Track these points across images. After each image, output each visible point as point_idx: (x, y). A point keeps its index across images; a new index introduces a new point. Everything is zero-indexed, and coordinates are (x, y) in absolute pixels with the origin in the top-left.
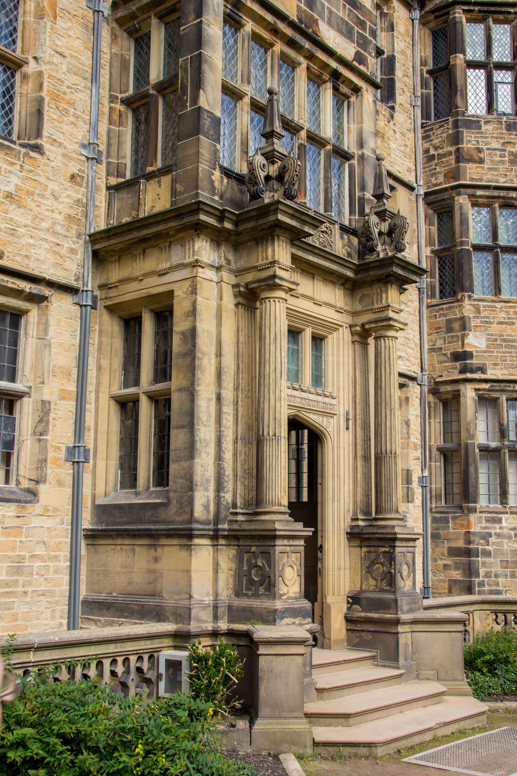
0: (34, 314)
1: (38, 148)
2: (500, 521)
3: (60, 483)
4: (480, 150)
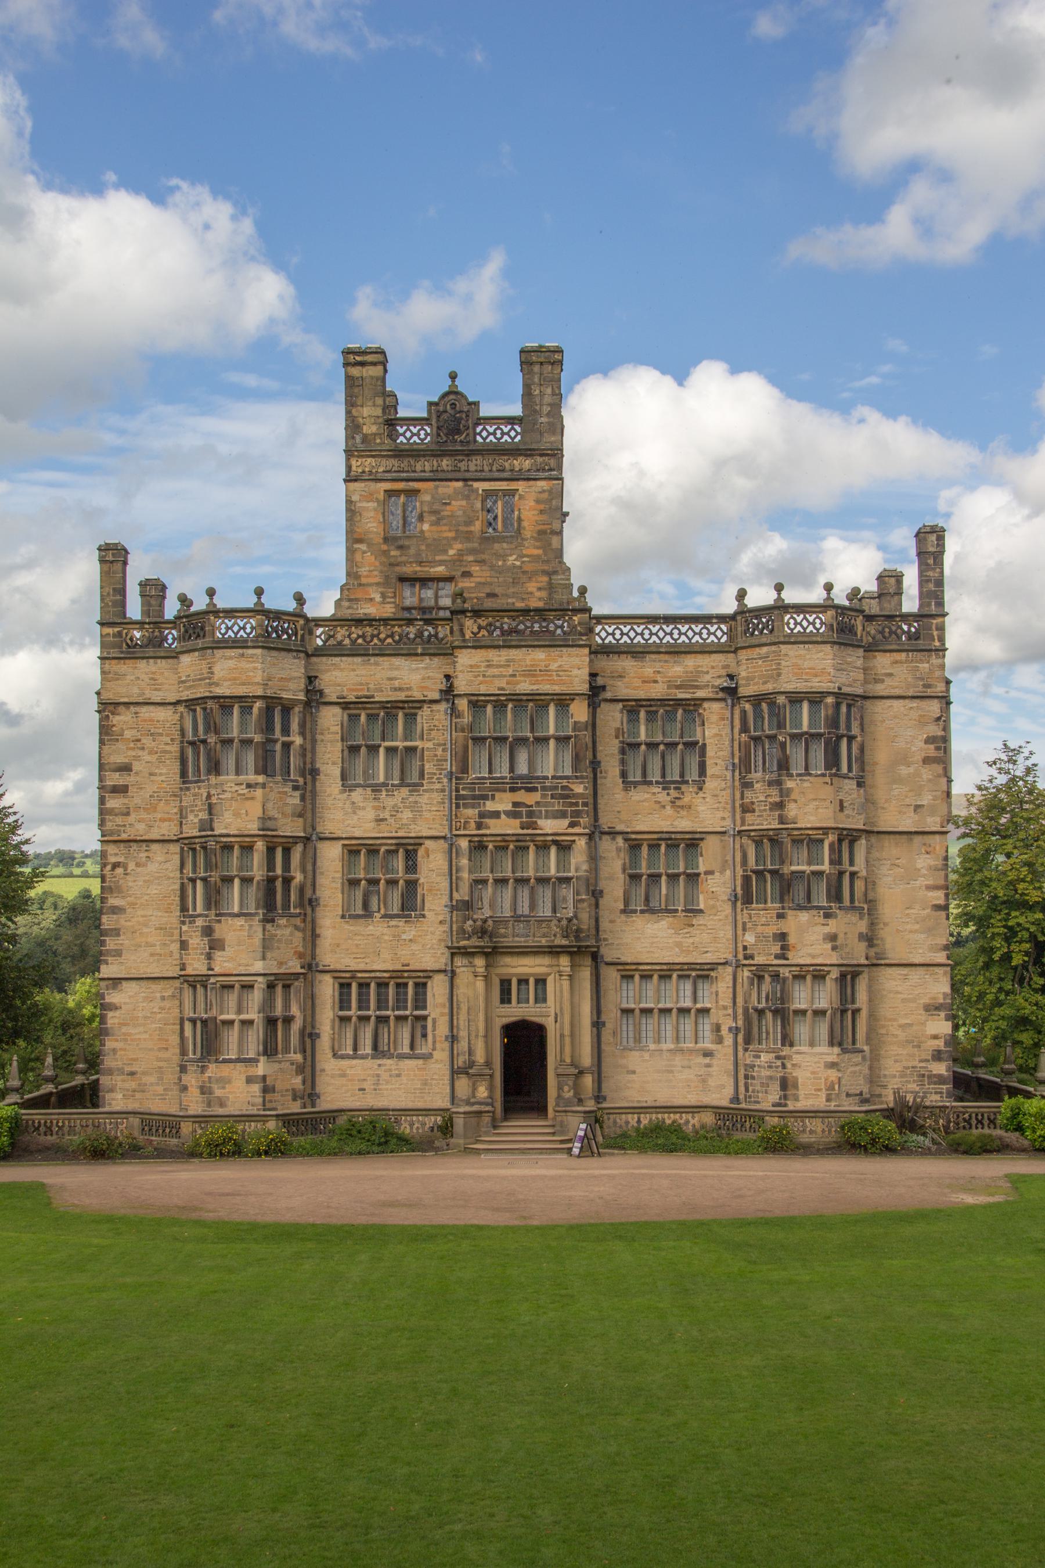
0: (429, 984)
1: (424, 916)
2: (759, 1057)
3: (443, 1050)
4: (753, 803)
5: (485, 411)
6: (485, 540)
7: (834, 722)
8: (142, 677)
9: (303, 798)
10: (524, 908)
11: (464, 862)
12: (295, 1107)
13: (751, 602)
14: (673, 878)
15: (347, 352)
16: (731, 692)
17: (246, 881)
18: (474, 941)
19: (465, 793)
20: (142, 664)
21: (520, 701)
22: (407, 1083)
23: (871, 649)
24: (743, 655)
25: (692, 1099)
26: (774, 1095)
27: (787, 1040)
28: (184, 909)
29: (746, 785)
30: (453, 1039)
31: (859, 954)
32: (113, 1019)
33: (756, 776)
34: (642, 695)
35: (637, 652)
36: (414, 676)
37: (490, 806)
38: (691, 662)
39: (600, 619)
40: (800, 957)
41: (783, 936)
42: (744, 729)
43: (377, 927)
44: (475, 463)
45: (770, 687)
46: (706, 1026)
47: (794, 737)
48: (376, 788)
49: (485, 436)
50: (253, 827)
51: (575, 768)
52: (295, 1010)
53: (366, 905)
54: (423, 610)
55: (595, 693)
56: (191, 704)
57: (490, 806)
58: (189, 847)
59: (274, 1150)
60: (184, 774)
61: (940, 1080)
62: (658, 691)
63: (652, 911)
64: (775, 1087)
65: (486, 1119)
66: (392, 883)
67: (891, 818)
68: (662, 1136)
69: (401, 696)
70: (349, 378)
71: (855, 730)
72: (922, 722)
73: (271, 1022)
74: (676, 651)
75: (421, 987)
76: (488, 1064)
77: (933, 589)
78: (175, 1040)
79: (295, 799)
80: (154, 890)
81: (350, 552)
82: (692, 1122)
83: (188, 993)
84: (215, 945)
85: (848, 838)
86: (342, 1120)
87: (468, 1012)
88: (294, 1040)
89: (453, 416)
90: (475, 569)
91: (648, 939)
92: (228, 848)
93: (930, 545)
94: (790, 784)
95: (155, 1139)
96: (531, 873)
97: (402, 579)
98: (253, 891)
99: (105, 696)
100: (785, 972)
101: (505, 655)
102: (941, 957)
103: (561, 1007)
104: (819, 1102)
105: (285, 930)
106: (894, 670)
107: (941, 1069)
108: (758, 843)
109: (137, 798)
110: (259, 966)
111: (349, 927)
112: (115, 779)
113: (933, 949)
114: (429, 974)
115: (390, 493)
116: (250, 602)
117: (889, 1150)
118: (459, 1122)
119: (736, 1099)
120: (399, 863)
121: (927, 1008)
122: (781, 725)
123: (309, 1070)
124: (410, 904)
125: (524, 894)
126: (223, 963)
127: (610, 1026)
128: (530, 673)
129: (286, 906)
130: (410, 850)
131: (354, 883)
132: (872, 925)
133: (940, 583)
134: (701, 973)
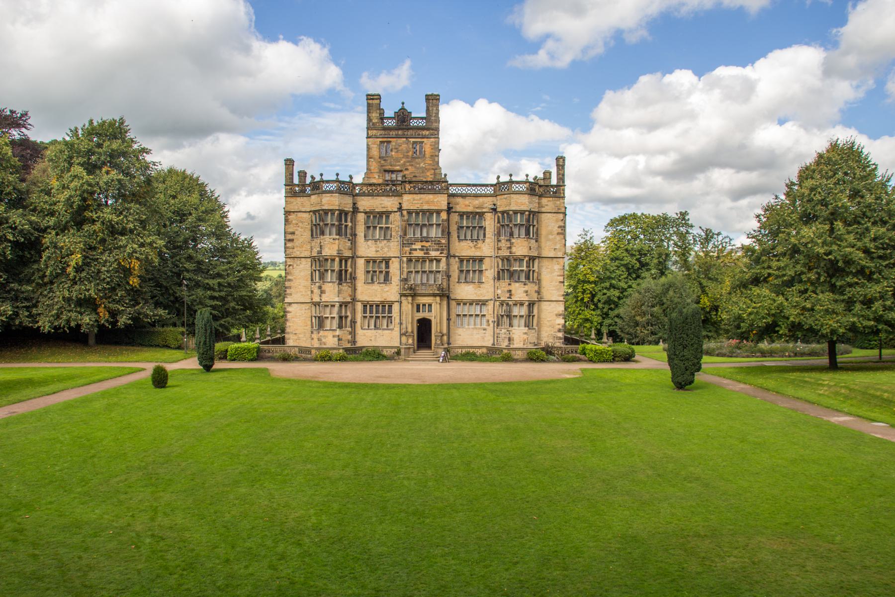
5: (413, 116)
6: (413, 158)
7: (528, 220)
8: (299, 203)
10: (425, 281)
11: (405, 265)
12: (349, 346)
13: (501, 180)
14: (474, 271)
15: (368, 95)
16: (494, 210)
17: (333, 271)
18: (408, 292)
19: (406, 243)
20: (298, 199)
21: (424, 212)
22: (386, 338)
23: (541, 196)
24: (498, 197)
25: (479, 344)
26: (506, 343)
27: (511, 325)
28: (312, 280)
29: (499, 241)
30: (401, 324)
31: (535, 297)
32: (289, 316)
33: (502, 238)
34: (465, 210)
35: (463, 196)
36: (388, 203)
37: (414, 247)
38: (481, 200)
39: (451, 185)
40: (516, 298)
41: (510, 291)
42: (499, 222)
43: (376, 287)
44: (410, 132)
45: (507, 209)
46: (484, 320)
47: (515, 225)
48: (376, 241)
49: (414, 123)
50: (335, 253)
51: (442, 234)
52: (349, 314)
53: (372, 279)
54: (392, 181)
55: (449, 210)
56: (314, 212)
57: (414, 247)
58: (314, 259)
59: (342, 359)
60: (312, 235)
61: (560, 338)
62: (470, 209)
63: (467, 282)
64: (507, 340)
65: (412, 350)
66: (381, 272)
67: (545, 253)
68: (469, 356)
69: (384, 210)
70: (368, 104)
71: (535, 223)
72: (557, 221)
73: (341, 318)
74: (476, 196)
75: (390, 306)
76: (412, 332)
77: (561, 178)
78: (309, 323)
79: (349, 244)
80: (302, 274)
81: (368, 161)
82: (479, 352)
83: (313, 307)
84: (323, 292)
85: (532, 259)
86: (364, 350)
87: (405, 315)
88: (348, 323)
89: (403, 117)
90: (410, 168)
91: (464, 291)
92: (326, 260)
93: (561, 162)
94: (513, 241)
95: (303, 355)
96: (427, 269)
97: (385, 171)
98: (335, 274)
99: (287, 209)
100: (510, 303)
101: (419, 196)
102: (561, 298)
103: (436, 314)
104: (521, 345)
105: (346, 288)
106: (548, 203)
107: (561, 335)
108: (503, 260)
109: (297, 243)
110: (337, 299)
111: (366, 286)
112: (290, 237)
113: (559, 296)
114: (393, 302)
115: (381, 142)
116: (334, 178)
117: (543, 361)
118: (403, 351)
119: (494, 344)
120: (383, 265)
121: (557, 315)
122: (511, 221)
123: (353, 333)
124: (387, 279)
125: (425, 276)
126: (325, 298)
127: (453, 320)
128: (427, 203)
129: (346, 279)
130: (387, 261)
131: (368, 272)
132: (539, 287)
133: (563, 175)
134: (483, 303)
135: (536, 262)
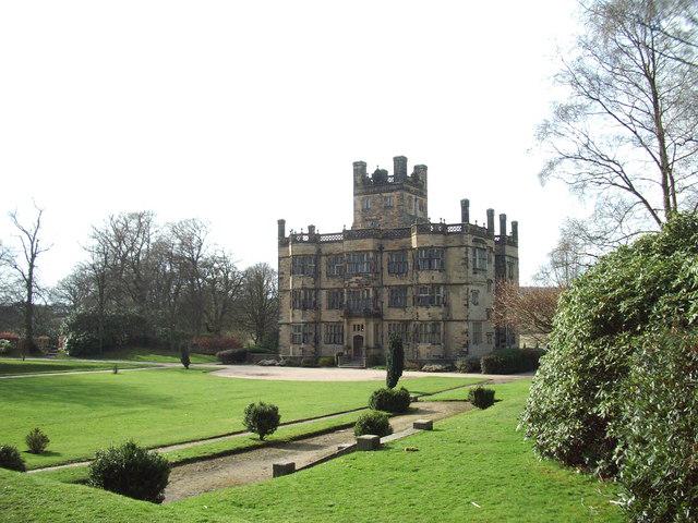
9: (315, 280)
31: (440, 317)
43: (334, 312)
55: (380, 250)
62: (396, 248)
73: (305, 334)
85: (435, 286)
91: (396, 314)
135: (442, 289)
